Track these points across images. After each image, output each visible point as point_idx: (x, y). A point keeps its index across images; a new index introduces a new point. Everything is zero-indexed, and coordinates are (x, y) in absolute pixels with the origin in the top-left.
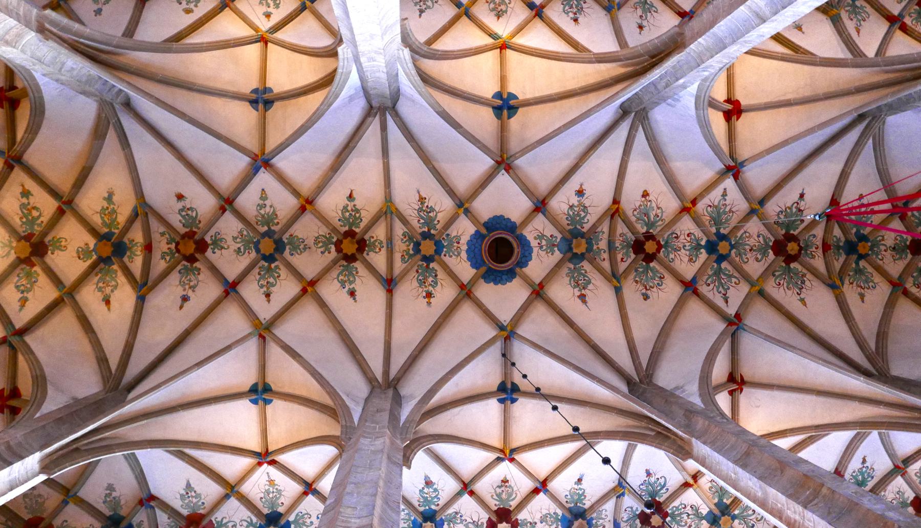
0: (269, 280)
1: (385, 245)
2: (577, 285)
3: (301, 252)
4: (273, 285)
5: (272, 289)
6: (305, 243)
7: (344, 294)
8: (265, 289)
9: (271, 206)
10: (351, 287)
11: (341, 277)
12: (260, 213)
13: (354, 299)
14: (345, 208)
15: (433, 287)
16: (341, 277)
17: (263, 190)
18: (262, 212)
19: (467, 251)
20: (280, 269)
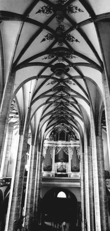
0: (45, 10)
1: (61, 46)
2: (51, 82)
3: (58, 21)
4: (43, 13)
5: (42, 12)
6: (61, 22)
7: (43, 37)
8: (41, 10)
9: (76, 12)
10: (46, 39)
11: (49, 35)
12: (73, 7)
13: (42, 41)
14: (73, 38)
15: (48, 58)
16: (49, 35)
17: (83, 11)
18: (74, 8)
19: (60, 63)
20: (50, 14)
